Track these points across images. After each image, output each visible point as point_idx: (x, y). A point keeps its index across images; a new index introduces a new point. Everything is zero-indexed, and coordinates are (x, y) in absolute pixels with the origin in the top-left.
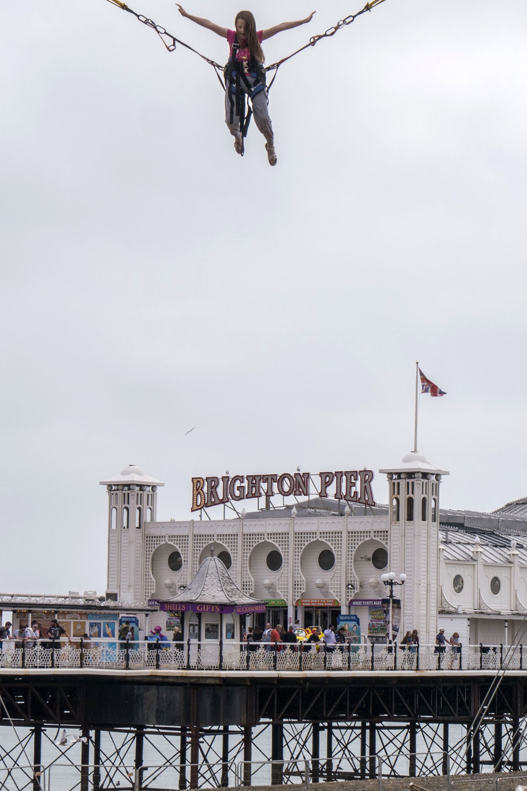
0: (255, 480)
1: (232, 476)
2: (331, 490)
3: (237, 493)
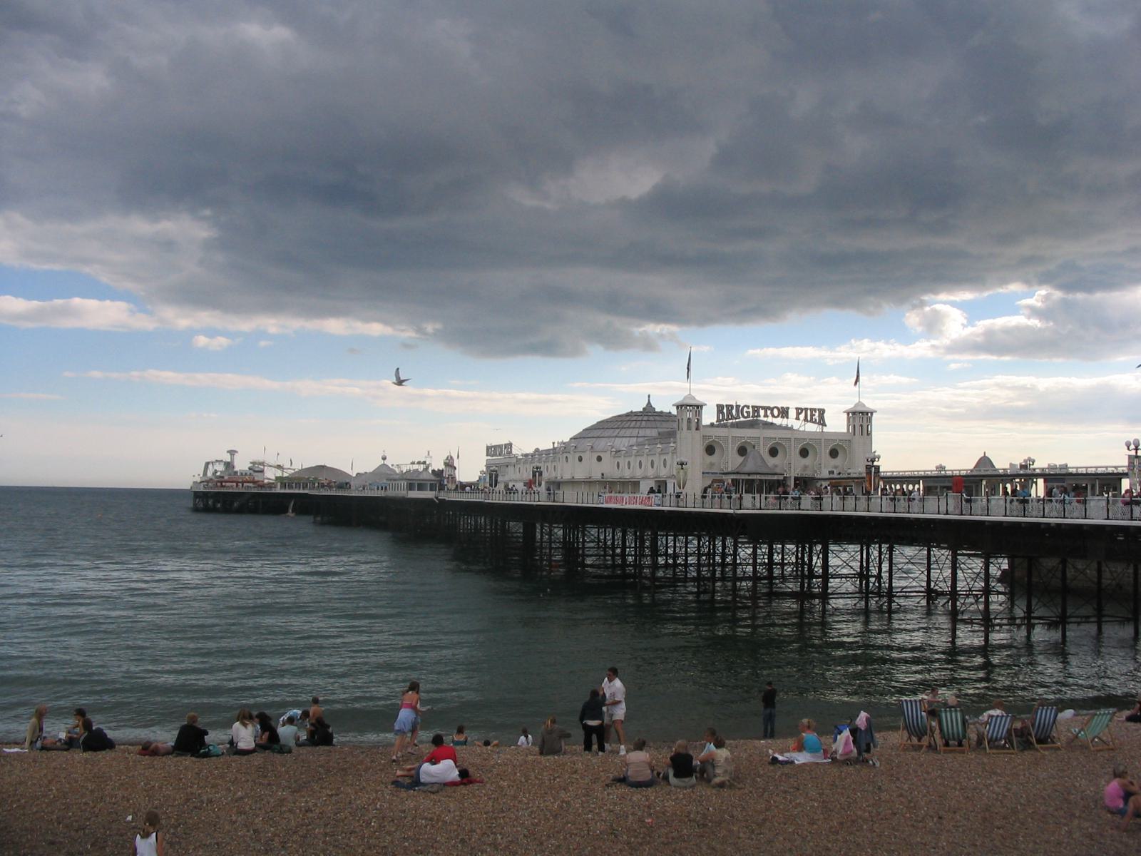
0: (756, 409)
1: (742, 405)
2: (802, 416)
3: (745, 415)
